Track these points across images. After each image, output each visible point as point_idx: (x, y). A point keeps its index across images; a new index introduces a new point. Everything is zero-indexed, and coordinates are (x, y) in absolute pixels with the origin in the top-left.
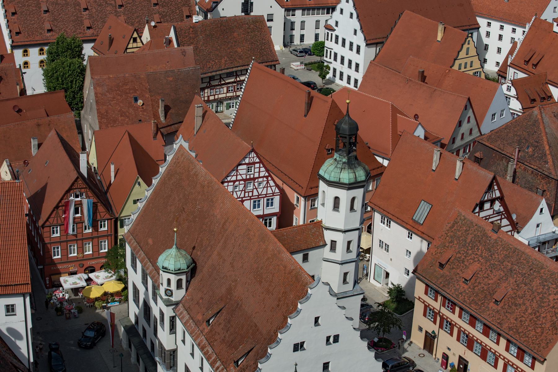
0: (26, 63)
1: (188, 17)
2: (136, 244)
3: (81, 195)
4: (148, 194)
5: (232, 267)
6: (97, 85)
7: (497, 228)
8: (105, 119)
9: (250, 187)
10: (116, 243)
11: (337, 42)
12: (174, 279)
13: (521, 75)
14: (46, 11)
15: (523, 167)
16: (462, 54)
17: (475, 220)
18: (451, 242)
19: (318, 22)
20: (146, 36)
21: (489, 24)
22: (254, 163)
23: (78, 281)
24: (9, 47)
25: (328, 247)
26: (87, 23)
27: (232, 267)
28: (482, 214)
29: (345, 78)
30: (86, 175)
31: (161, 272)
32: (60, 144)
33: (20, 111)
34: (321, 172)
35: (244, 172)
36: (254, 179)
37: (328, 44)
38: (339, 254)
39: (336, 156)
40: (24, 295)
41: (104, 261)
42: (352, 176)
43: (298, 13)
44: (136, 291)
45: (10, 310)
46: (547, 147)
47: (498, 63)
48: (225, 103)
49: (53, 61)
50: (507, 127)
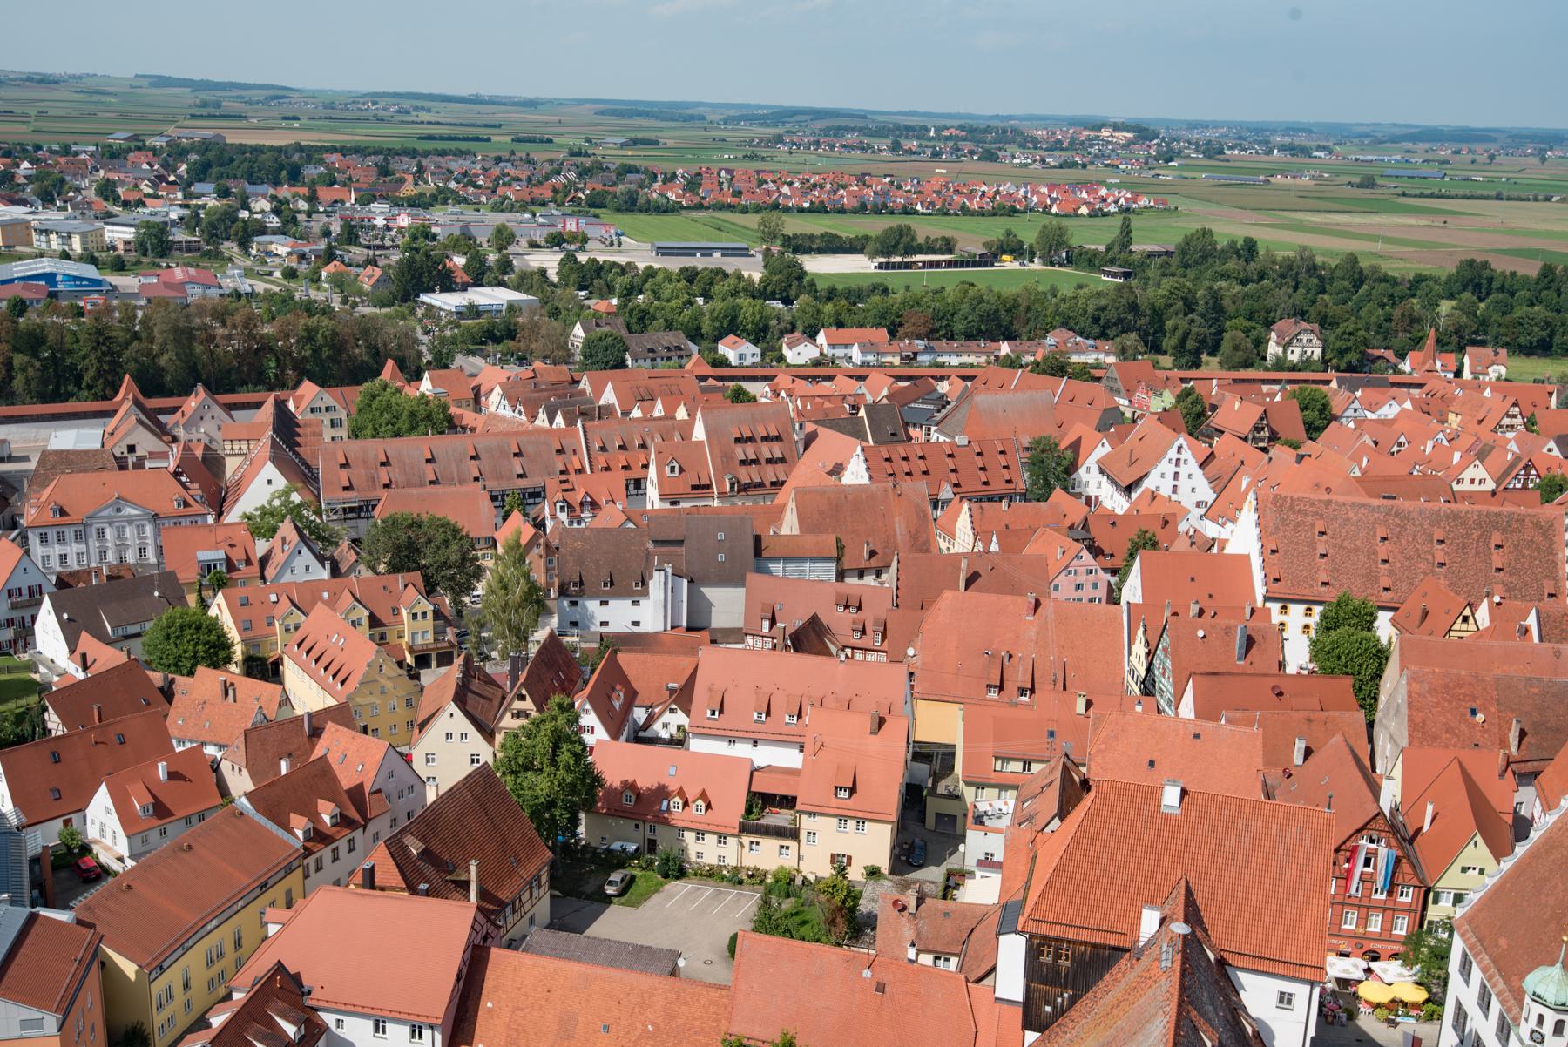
1: (1551, 595)
2: (1474, 939)
4: (1507, 864)
8: (1420, 732)
10: (1421, 925)
12: (1551, 1018)
14: (1324, 556)
20: (1483, 614)
23: (1352, 969)
26: (1385, 582)
31: (1527, 1000)
32: (1350, 757)
33: (1280, 694)
40: (1312, 984)
41: (1396, 948)
44: (1461, 1015)
45: (1285, 999)
49: (1328, 629)
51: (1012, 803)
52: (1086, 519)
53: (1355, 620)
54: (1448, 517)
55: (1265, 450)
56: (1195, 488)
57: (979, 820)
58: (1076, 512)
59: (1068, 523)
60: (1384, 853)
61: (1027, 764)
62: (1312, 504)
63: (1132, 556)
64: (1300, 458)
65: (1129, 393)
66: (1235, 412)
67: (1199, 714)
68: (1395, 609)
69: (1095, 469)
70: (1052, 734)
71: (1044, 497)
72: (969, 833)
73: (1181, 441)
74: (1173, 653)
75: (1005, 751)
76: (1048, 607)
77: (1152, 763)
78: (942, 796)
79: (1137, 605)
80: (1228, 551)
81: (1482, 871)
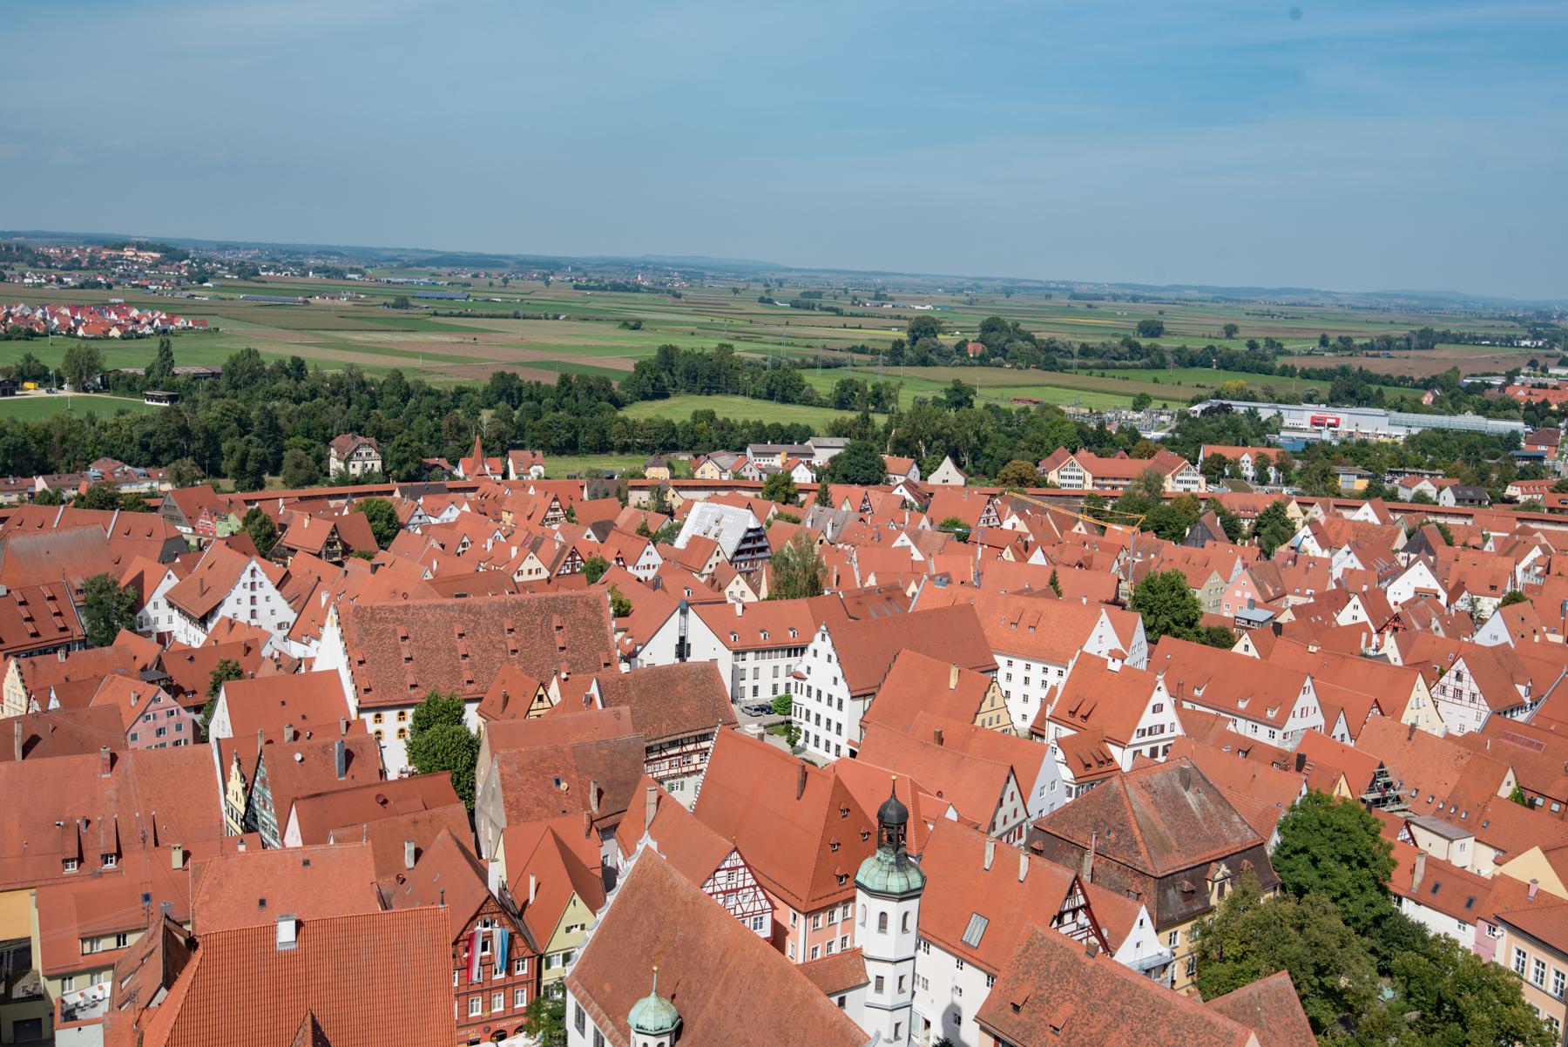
0: (378, 733)
1: (607, 665)
3: (493, 922)
4: (602, 915)
5: (741, 1020)
6: (504, 762)
7: (1091, 952)
8: (516, 812)
9: (732, 902)
11: (809, 695)
13: (1066, 732)
15: (1104, 860)
16: (986, 706)
17: (1059, 940)
18: (1027, 972)
19: (776, 668)
20: (554, 691)
21: (1010, 663)
22: (737, 868)
24: (353, 711)
25: (872, 985)
26: (467, 676)
27: (741, 1020)
28: (1063, 930)
29: (822, 743)
30: (496, 894)
31: (633, 1033)
33: (385, 802)
34: (860, 878)
35: (724, 880)
36: (737, 890)
37: (796, 698)
38: (889, 996)
39: (879, 854)
41: (519, 1021)
42: (903, 881)
43: (750, 656)
46: (1137, 832)
47: (1024, 717)
48: (667, 783)
49: (422, 729)
50: (1074, 805)
51: (108, 986)
52: (160, 658)
53: (446, 716)
54: (513, 607)
55: (340, 564)
56: (274, 610)
57: (70, 1016)
58: (147, 651)
59: (139, 664)
60: (498, 933)
61: (121, 937)
62: (392, 611)
63: (216, 689)
64: (375, 568)
65: (191, 521)
66: (305, 529)
67: (305, 842)
68: (479, 700)
69: (163, 603)
70: (147, 898)
71: (108, 641)
72: (57, 1033)
73: (254, 564)
74: (273, 783)
75: (90, 930)
76: (126, 761)
77: (262, 902)
78: (20, 1000)
79: (227, 740)
80: (316, 668)
81: (583, 927)
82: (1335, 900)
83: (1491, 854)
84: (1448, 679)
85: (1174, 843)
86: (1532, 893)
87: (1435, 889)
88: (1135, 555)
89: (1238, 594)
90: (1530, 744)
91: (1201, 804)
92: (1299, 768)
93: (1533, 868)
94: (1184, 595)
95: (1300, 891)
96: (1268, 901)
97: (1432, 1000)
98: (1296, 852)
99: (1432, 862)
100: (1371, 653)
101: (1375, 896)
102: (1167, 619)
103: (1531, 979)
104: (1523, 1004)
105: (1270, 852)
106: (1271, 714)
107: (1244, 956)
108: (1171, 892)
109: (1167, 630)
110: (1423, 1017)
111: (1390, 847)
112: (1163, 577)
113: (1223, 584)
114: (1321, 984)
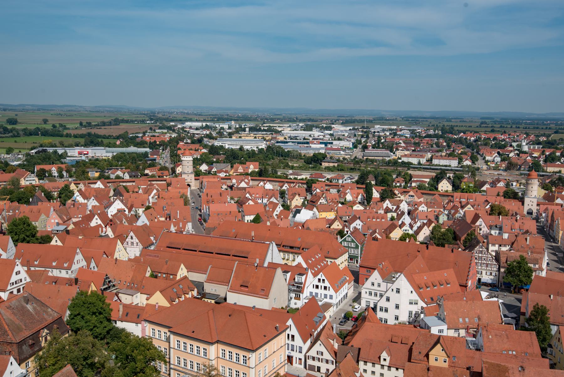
46: (6, 327)
82: (91, 330)
83: (145, 296)
84: (129, 239)
85: (24, 327)
86: (157, 307)
87: (127, 315)
88: (9, 212)
89: (53, 221)
90: (155, 256)
91: (34, 308)
92: (76, 284)
93: (159, 299)
94: (29, 225)
95: (76, 331)
96: (65, 338)
97: (124, 357)
98: (75, 316)
99: (125, 306)
100: (103, 234)
101: (106, 323)
102: (23, 236)
103: (157, 337)
104: (153, 347)
105: (66, 318)
106: (66, 265)
107: (56, 363)
108: (24, 347)
109: (23, 240)
110: (122, 363)
111: (109, 305)
112: (19, 219)
113: (47, 218)
114: (87, 363)
